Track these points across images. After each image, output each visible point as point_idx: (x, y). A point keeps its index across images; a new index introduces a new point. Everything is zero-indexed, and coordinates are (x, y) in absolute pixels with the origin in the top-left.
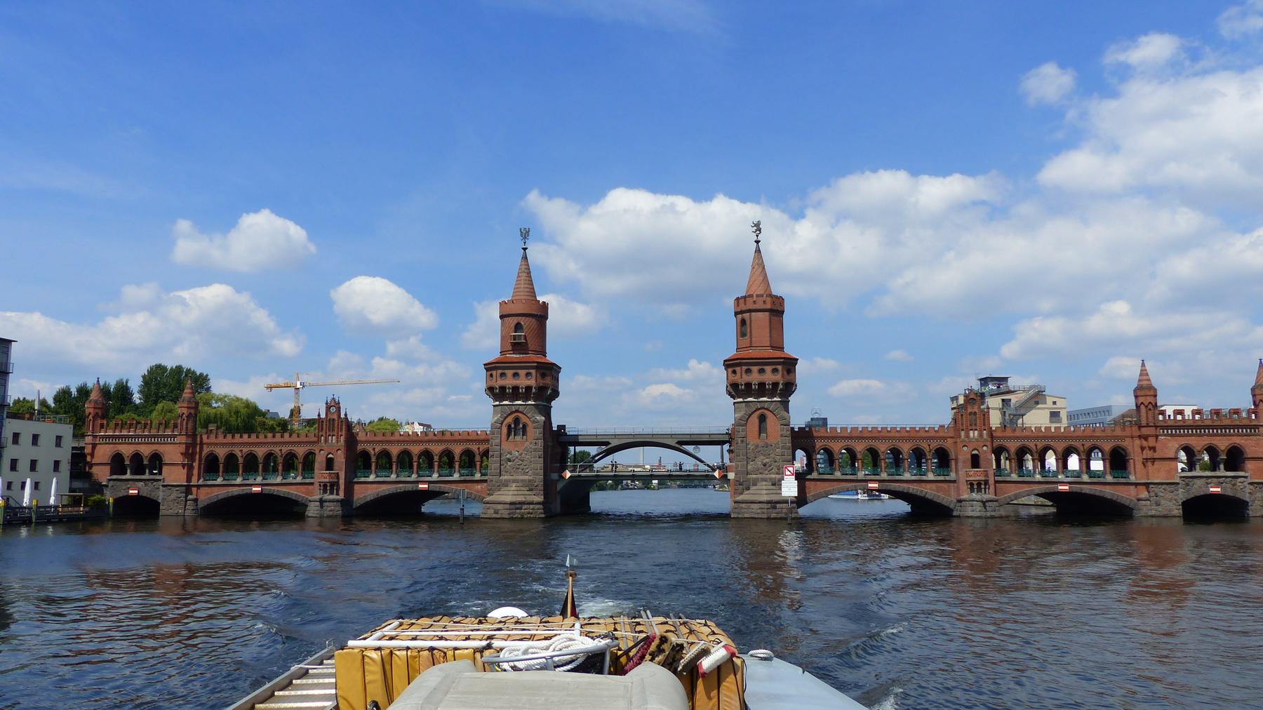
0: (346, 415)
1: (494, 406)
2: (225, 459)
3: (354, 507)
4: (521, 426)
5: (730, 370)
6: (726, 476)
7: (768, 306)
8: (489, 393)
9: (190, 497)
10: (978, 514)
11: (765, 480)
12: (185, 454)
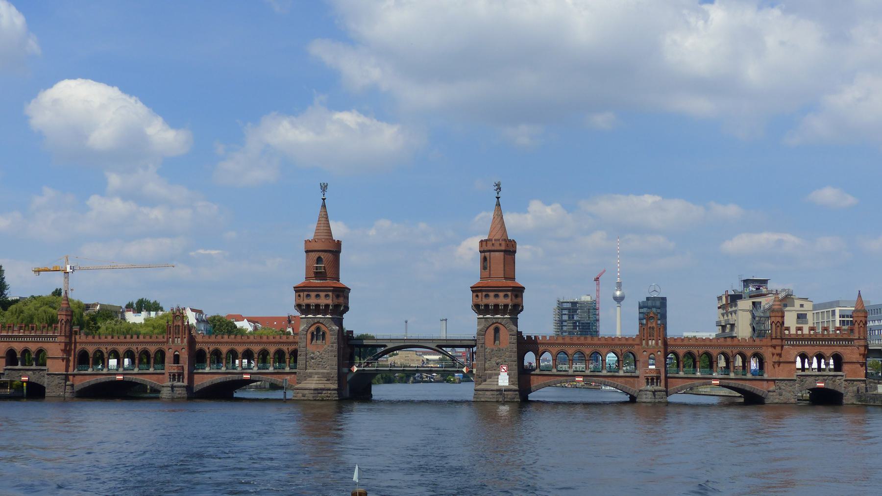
3: (194, 391)
4: (321, 333)
5: (475, 294)
6: (472, 371)
7: (503, 248)
8: (296, 308)
9: (68, 383)
10: (649, 400)
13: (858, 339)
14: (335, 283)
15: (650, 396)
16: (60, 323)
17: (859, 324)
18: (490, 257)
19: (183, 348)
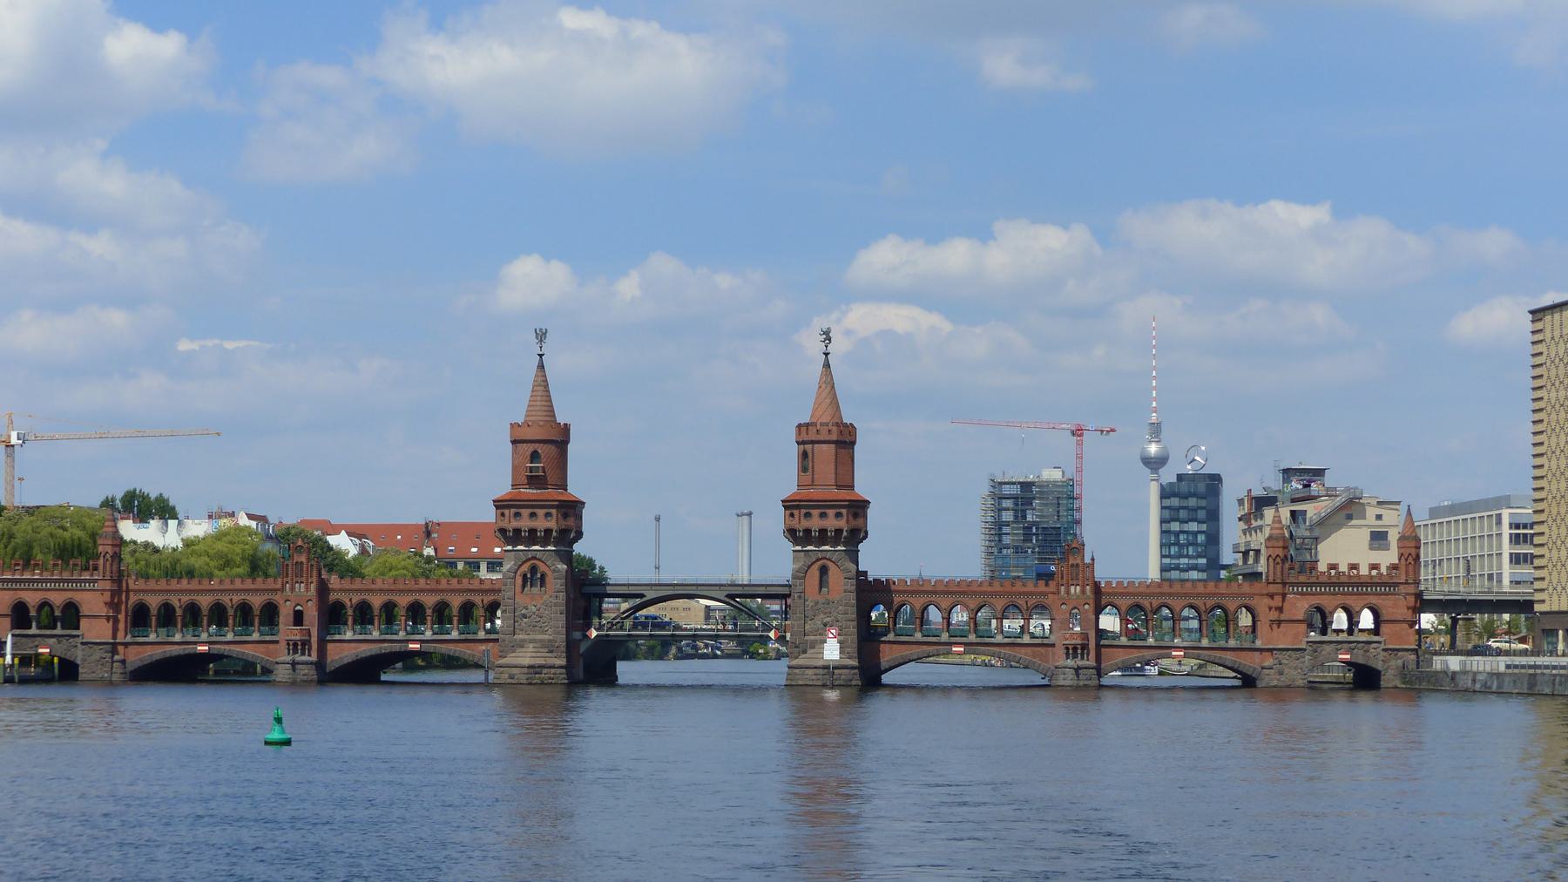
4: (539, 575)
5: (788, 512)
6: (784, 637)
7: (834, 437)
9: (116, 657)
10: (1068, 683)
12: (110, 604)
13: (1406, 583)
14: (562, 493)
16: (102, 558)
17: (1406, 560)
18: (813, 451)
19: (309, 600)
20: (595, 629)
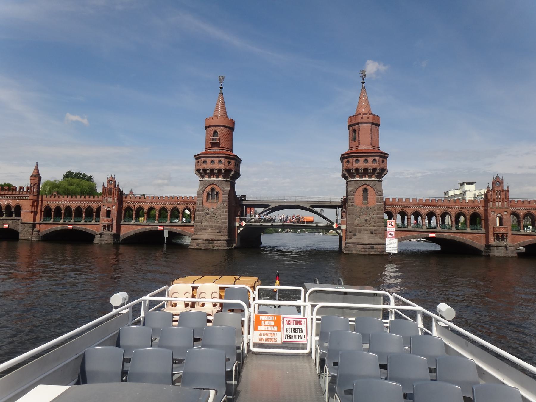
0: (118, 185)
1: (200, 181)
2: (75, 210)
4: (215, 193)
7: (370, 120)
8: (197, 172)
11: (365, 230)
15: (503, 251)
20: (245, 221)
